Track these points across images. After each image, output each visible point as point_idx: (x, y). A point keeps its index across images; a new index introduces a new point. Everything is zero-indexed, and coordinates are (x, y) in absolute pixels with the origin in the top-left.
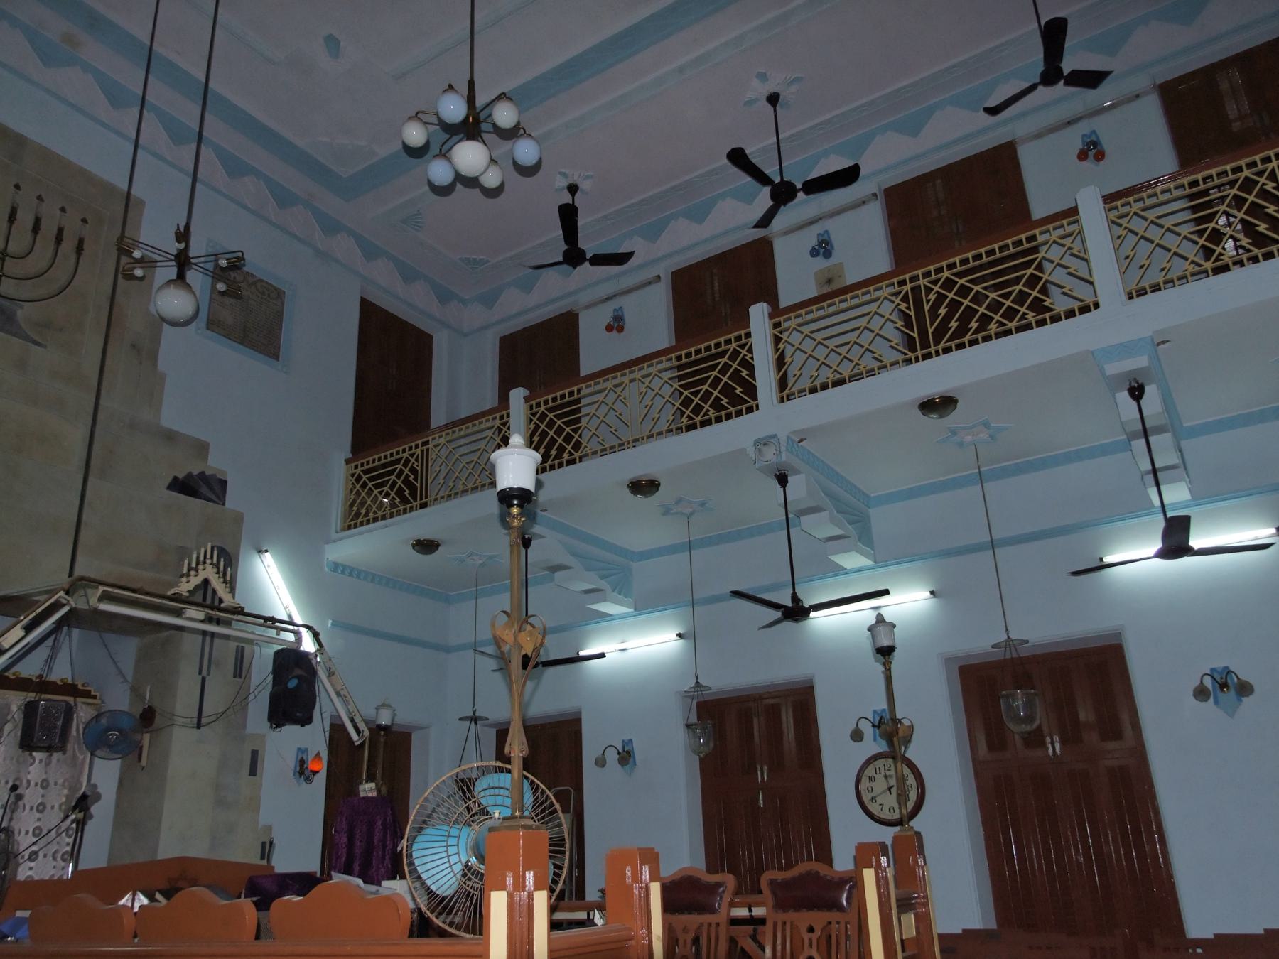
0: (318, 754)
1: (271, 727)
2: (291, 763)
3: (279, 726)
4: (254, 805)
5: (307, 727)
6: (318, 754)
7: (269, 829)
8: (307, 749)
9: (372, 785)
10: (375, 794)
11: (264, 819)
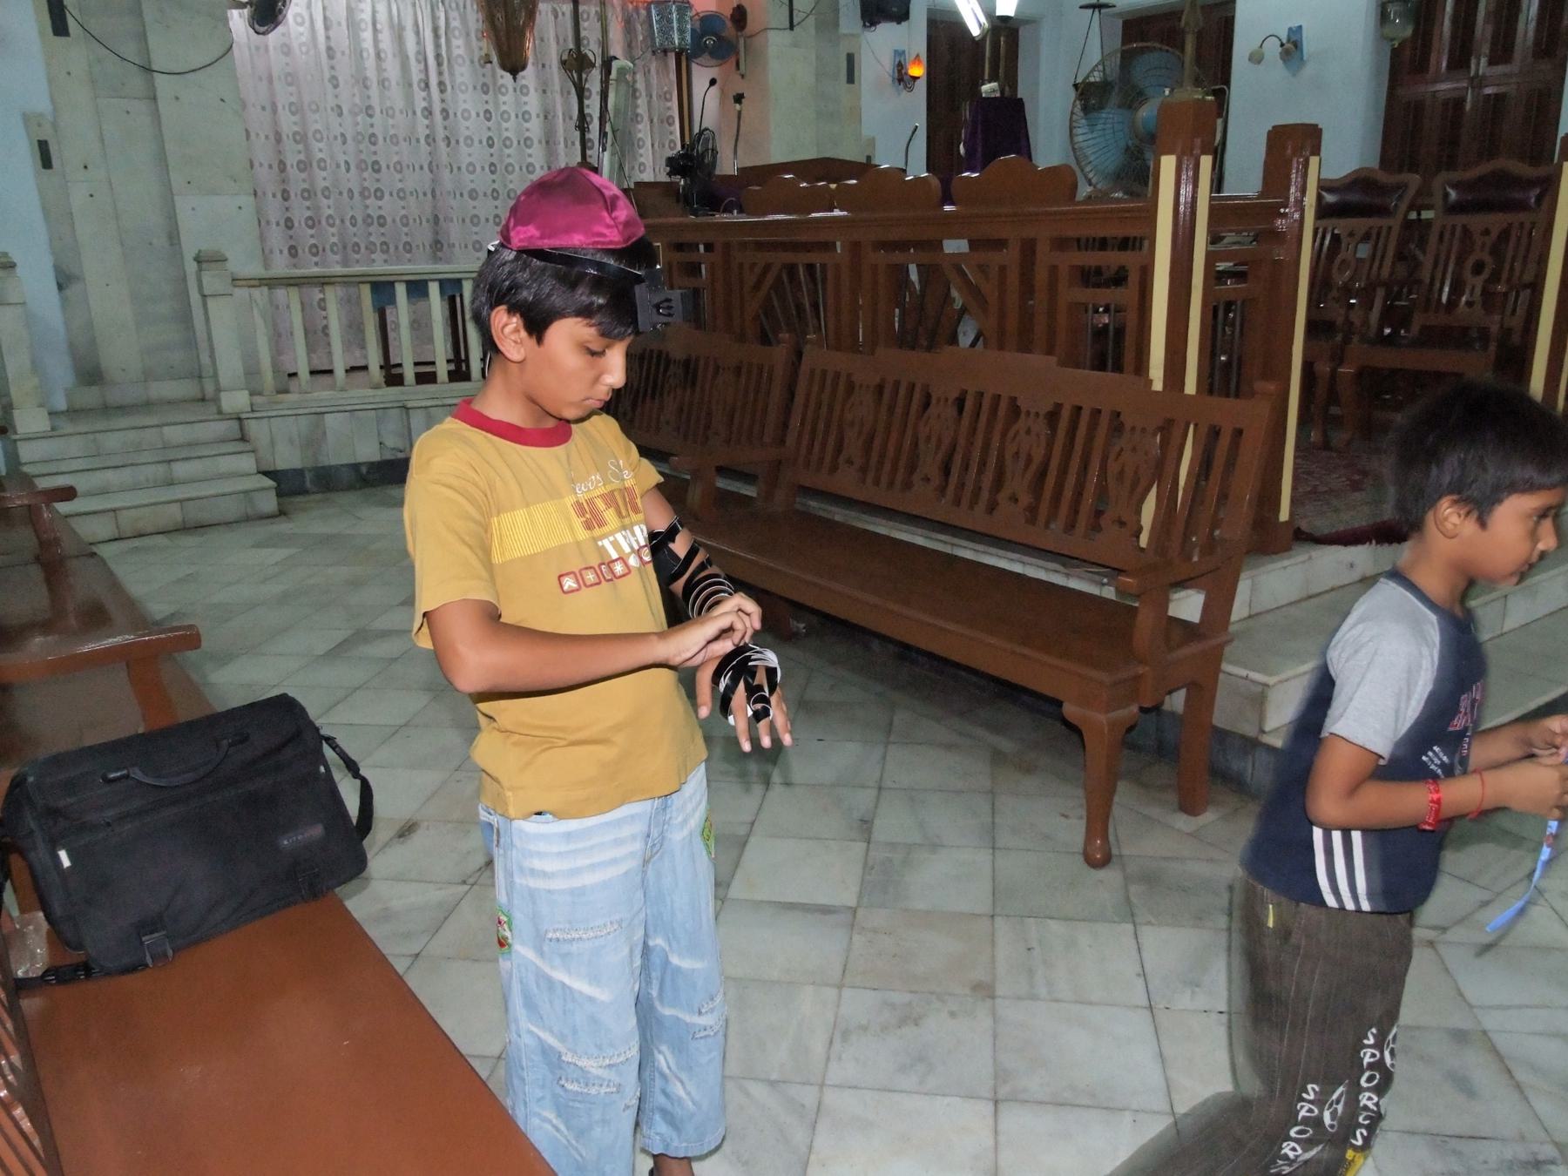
0: (918, 56)
1: (864, 25)
2: (888, 64)
3: (873, 24)
4: (855, 114)
5: (904, 24)
6: (918, 56)
7: (872, 142)
8: (904, 52)
9: (994, 85)
10: (998, 95)
11: (867, 131)
